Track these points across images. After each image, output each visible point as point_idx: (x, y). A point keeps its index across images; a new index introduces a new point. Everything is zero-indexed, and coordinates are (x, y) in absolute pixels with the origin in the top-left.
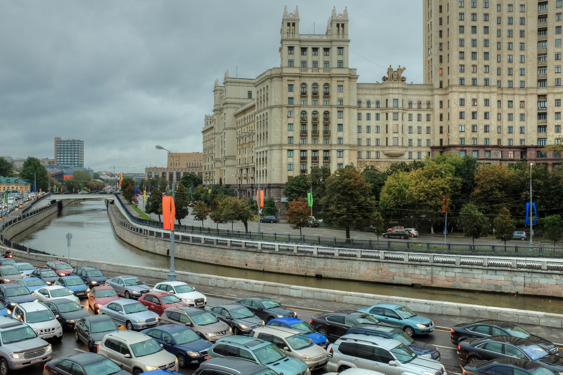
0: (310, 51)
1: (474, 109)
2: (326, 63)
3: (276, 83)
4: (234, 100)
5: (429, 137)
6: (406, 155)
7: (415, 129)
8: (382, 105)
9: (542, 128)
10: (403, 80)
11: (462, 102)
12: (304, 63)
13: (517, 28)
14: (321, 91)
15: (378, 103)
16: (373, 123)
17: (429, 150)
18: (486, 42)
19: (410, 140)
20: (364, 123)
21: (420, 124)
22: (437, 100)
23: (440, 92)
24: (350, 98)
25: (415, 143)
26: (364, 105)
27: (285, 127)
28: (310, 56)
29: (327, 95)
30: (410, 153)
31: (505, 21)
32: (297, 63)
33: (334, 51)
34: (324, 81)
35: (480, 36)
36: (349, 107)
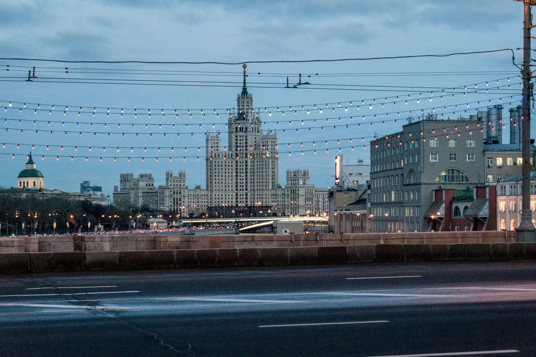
0: (176, 181)
1: (219, 197)
2: (180, 184)
3: (167, 190)
4: (142, 187)
5: (207, 204)
6: (201, 209)
7: (203, 202)
8: (195, 195)
9: (237, 202)
10: (200, 188)
11: (216, 195)
12: (174, 185)
13: (230, 174)
14: (179, 192)
15: (193, 195)
16: (192, 200)
17: (207, 207)
18: (222, 179)
19: (202, 205)
20: (190, 200)
21: (205, 200)
22: (209, 194)
23: (210, 192)
24: (186, 193)
25: (203, 205)
26: (190, 195)
27: (170, 202)
28: (176, 183)
29: (180, 193)
30: (202, 209)
31: (227, 173)
32: (172, 185)
33: (182, 181)
34: (180, 189)
35: (220, 177)
36: (186, 196)
